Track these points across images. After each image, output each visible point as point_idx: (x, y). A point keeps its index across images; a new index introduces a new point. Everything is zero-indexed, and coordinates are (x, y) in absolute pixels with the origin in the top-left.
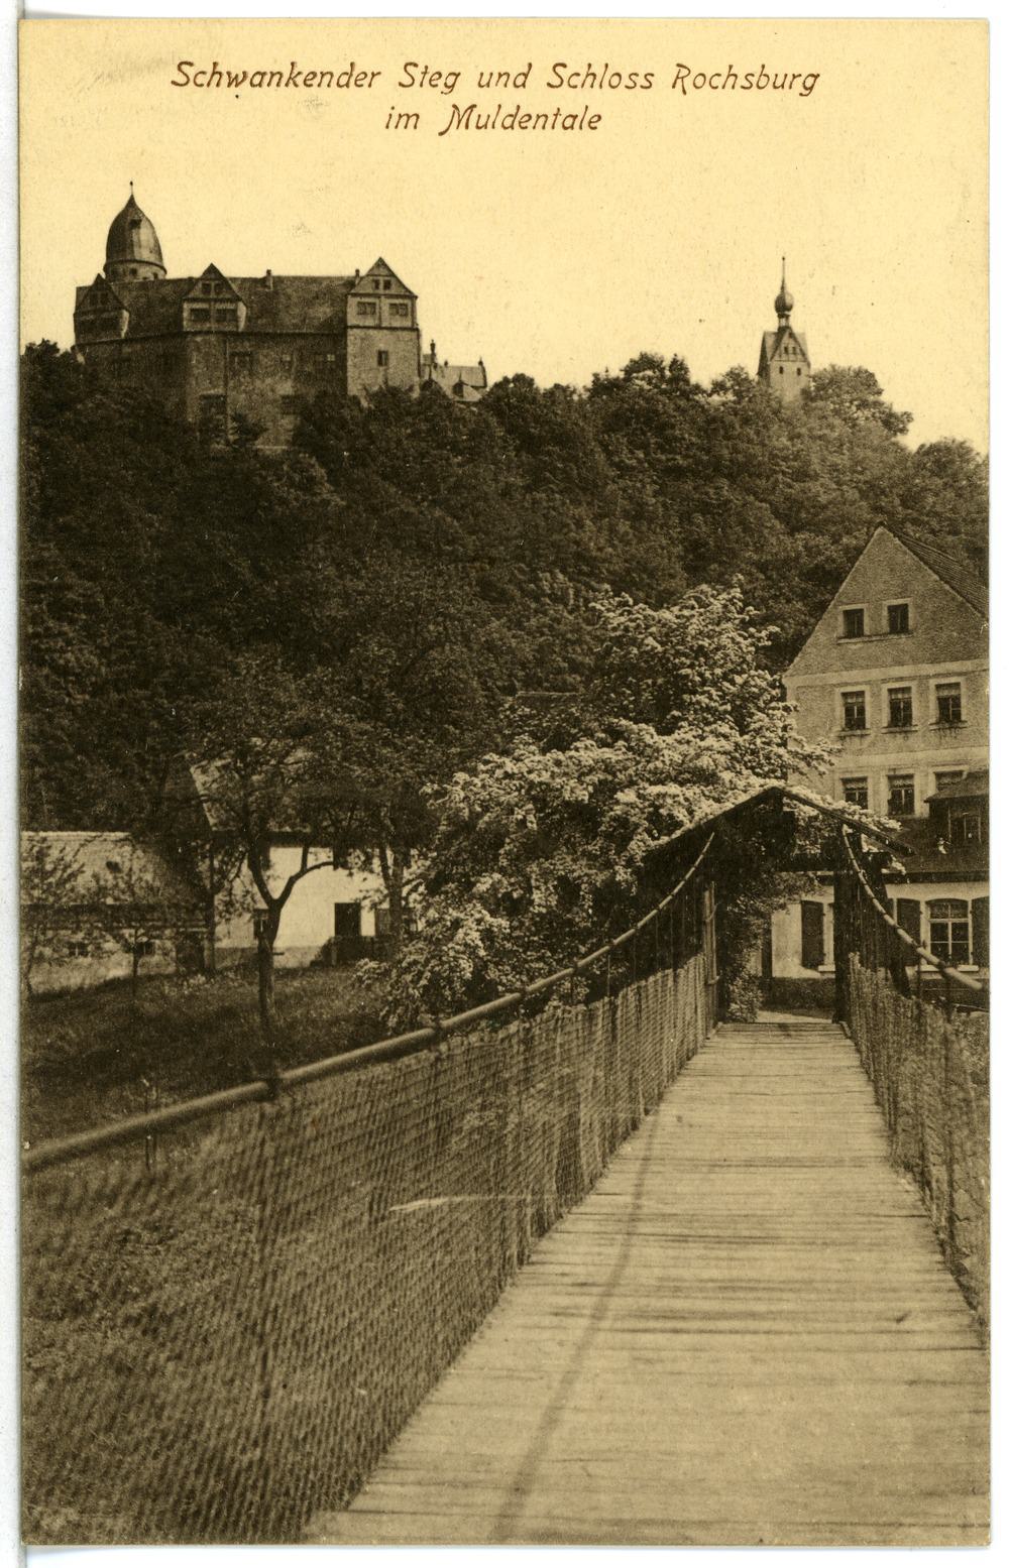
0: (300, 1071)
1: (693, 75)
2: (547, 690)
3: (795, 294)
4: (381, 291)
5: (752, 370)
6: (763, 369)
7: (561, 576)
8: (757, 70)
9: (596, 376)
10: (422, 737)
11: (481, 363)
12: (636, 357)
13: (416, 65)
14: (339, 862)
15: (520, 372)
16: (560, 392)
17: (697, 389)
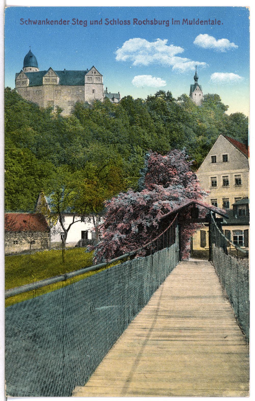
0: (73, 273)
1: (138, 21)
2: (136, 176)
3: (199, 76)
4: (93, 74)
5: (188, 95)
6: (191, 95)
7: (139, 147)
8: (153, 20)
9: (148, 96)
10: (104, 189)
11: (119, 93)
12: (158, 91)
13: (75, 19)
14: (82, 220)
15: (129, 95)
16: (139, 100)
17: (174, 99)
